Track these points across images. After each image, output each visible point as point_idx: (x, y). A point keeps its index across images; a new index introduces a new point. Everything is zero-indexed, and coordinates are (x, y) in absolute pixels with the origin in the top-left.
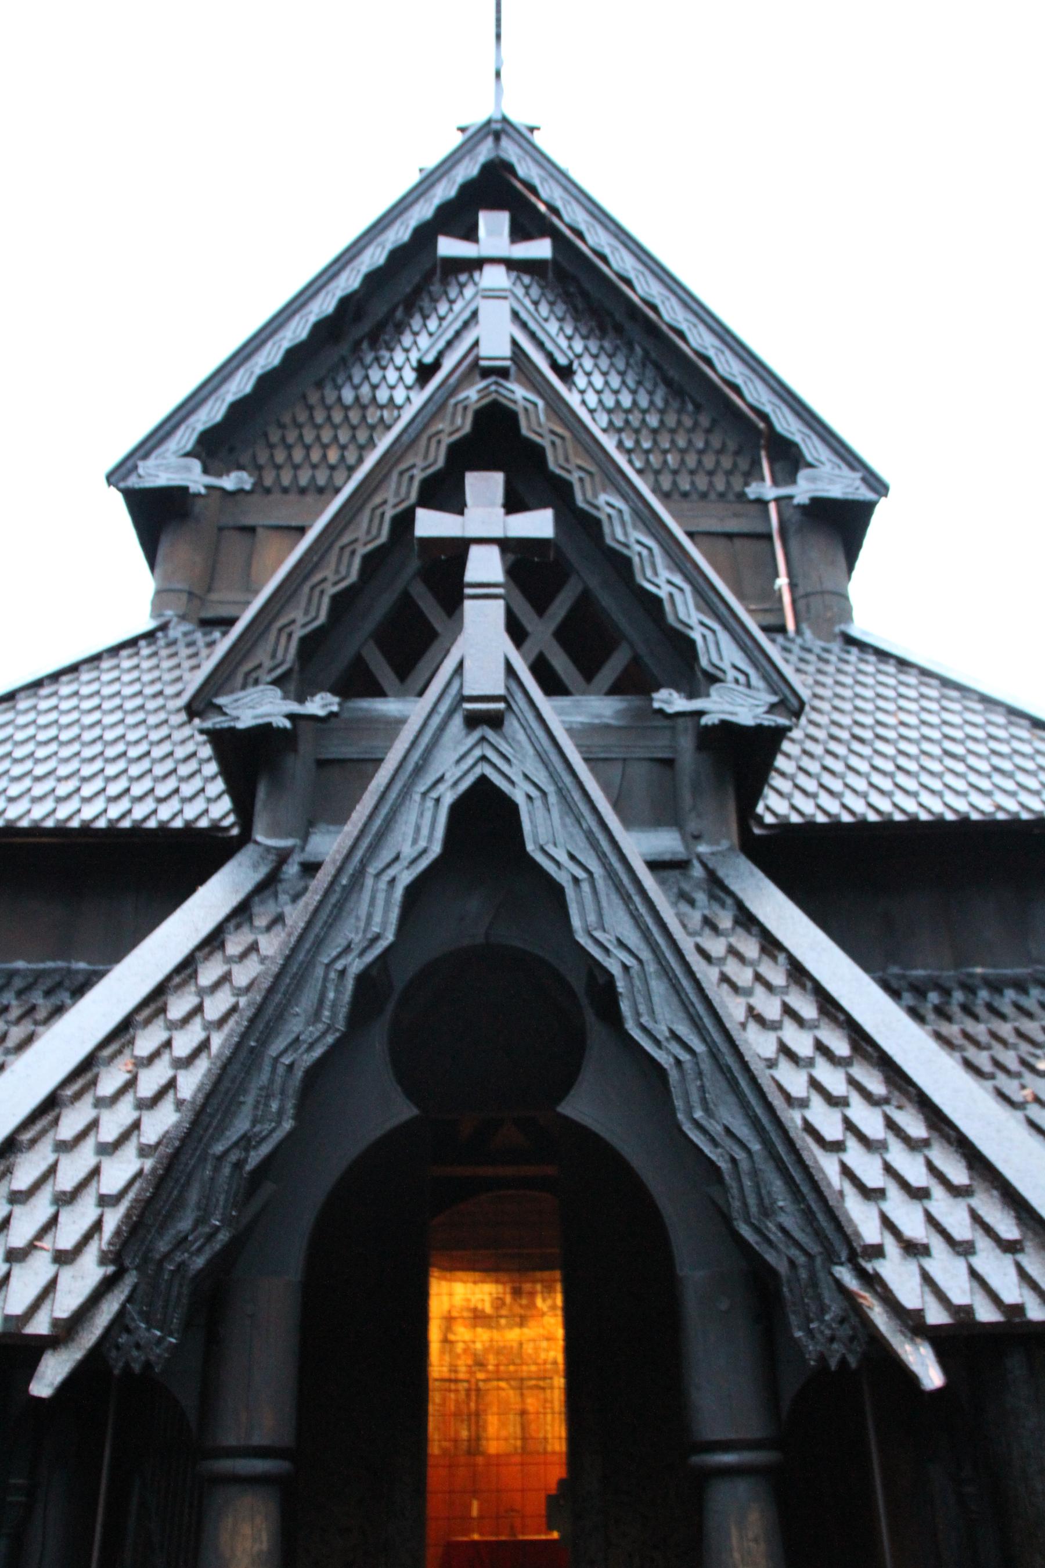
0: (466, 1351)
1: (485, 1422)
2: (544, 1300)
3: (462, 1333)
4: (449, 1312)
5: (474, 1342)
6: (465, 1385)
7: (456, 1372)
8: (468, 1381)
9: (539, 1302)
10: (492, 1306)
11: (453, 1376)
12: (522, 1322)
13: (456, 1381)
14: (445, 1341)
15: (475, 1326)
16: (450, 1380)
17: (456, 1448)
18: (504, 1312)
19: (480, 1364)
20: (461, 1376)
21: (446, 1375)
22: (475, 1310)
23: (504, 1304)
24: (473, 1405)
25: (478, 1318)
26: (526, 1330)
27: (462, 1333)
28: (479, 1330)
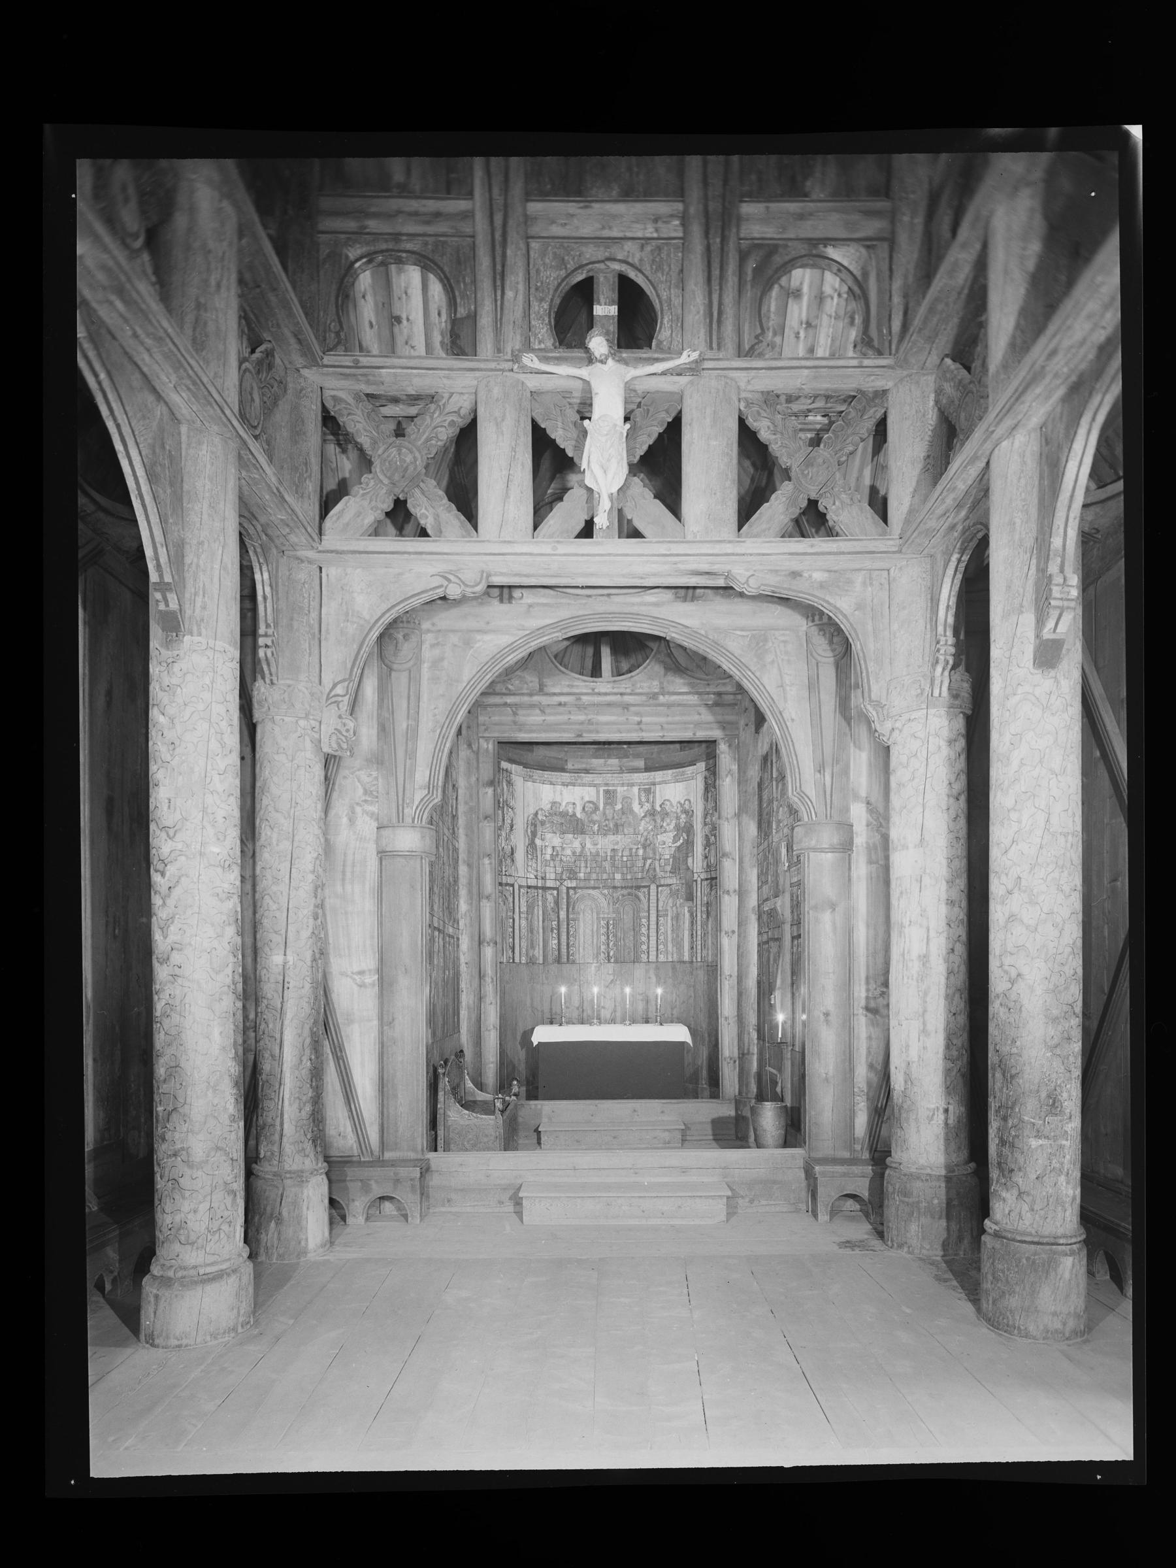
0: (553, 858)
2: (641, 804)
3: (551, 840)
4: (536, 814)
5: (563, 849)
6: (555, 892)
9: (636, 807)
12: (617, 829)
13: (544, 888)
14: (532, 844)
16: (536, 888)
17: (545, 957)
18: (595, 817)
19: (573, 874)
20: (549, 884)
21: (532, 882)
22: (564, 814)
23: (597, 808)
24: (563, 914)
27: (551, 840)
28: (571, 836)
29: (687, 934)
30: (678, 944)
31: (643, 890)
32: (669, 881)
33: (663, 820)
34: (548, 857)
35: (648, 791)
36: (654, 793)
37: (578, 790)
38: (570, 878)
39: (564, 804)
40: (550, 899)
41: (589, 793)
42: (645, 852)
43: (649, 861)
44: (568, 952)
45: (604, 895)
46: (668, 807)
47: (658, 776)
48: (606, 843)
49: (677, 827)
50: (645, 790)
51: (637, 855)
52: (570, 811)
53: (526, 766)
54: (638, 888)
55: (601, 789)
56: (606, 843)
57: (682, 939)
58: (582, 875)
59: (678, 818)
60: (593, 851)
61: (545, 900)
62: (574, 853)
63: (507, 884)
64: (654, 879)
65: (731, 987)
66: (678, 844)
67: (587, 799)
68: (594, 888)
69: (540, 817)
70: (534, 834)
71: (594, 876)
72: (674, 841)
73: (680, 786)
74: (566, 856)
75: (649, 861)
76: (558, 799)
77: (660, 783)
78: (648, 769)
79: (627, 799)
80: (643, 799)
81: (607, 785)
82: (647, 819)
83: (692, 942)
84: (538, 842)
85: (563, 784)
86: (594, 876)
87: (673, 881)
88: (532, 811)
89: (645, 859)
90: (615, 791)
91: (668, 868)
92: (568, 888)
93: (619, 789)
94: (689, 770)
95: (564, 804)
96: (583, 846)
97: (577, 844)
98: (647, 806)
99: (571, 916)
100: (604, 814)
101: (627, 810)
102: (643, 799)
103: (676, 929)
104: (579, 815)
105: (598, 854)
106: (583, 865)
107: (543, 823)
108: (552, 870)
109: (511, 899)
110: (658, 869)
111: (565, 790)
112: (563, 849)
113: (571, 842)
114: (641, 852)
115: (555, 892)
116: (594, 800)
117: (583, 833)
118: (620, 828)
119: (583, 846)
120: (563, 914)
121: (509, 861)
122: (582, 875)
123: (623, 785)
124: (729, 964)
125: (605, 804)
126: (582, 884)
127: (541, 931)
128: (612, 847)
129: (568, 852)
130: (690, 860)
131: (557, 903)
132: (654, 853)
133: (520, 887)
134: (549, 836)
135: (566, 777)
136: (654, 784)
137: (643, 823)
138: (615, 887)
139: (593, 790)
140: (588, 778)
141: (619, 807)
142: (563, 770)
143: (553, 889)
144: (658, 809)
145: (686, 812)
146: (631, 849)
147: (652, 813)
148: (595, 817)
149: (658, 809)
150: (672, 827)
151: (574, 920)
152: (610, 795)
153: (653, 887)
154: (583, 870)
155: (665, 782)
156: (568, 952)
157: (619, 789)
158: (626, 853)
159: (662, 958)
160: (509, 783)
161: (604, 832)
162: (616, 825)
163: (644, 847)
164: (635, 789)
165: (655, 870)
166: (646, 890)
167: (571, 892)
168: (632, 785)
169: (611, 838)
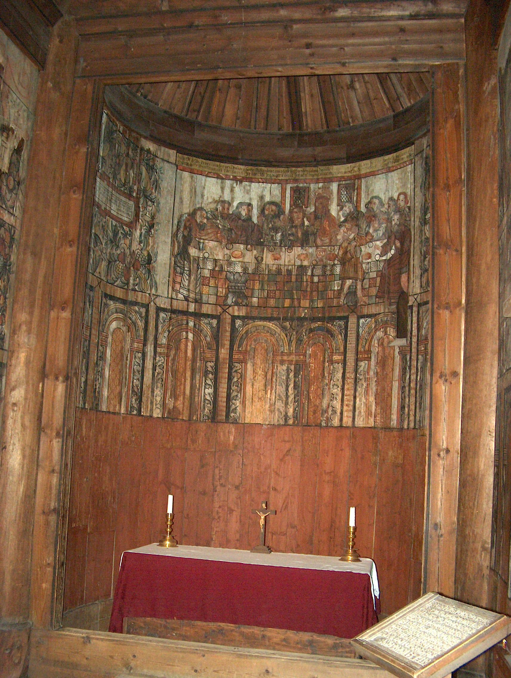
1: (243, 377)
2: (341, 206)
4: (192, 214)
5: (230, 263)
6: (214, 322)
7: (198, 301)
8: (218, 318)
9: (334, 210)
10: (262, 211)
11: (192, 308)
13: (198, 315)
15: (232, 242)
16: (185, 313)
19: (241, 295)
20: (206, 309)
21: (179, 305)
23: (280, 211)
24: (224, 352)
25: (239, 229)
26: (311, 250)
27: (213, 250)
28: (242, 246)
29: (396, 385)
30: (383, 399)
31: (337, 323)
32: (373, 310)
33: (369, 226)
34: (206, 273)
35: (351, 185)
36: (359, 188)
37: (256, 189)
38: (236, 304)
39: (235, 204)
40: (207, 330)
41: (270, 192)
42: (343, 270)
43: (348, 282)
44: (228, 407)
45: (284, 328)
46: (376, 207)
47: (365, 166)
48: (290, 258)
49: (390, 236)
50: (346, 187)
51: (332, 274)
52: (244, 213)
53: (181, 150)
54: (332, 319)
55: (289, 187)
56: (290, 258)
57: (390, 395)
58: (255, 300)
59: (389, 220)
60: (274, 268)
61: (197, 331)
62: (245, 269)
63: (136, 303)
64: (354, 308)
65: (448, 472)
66: (389, 255)
67: (267, 199)
68: (270, 319)
69: (198, 221)
70: (187, 241)
71: (272, 302)
72: (384, 252)
73: (395, 176)
74: (234, 274)
75: (348, 282)
76: (227, 197)
77: (367, 175)
78: (351, 159)
79: (323, 201)
80: (344, 199)
81: (296, 181)
82: (348, 225)
83: (403, 399)
84: (193, 252)
85: (235, 179)
86: (272, 302)
87: (381, 309)
88: (187, 209)
89: (343, 279)
90: (309, 188)
91: (374, 291)
92: (234, 318)
93: (312, 186)
94: (405, 153)
95: (235, 204)
96: (259, 260)
97: (250, 257)
98: (348, 208)
99: (236, 356)
100: (291, 220)
101: (322, 213)
102: (344, 199)
103: (383, 378)
104: (255, 220)
105: (279, 272)
106: (257, 286)
107: (202, 227)
108: (212, 291)
109: (141, 324)
110: (359, 293)
111: (238, 189)
112: (230, 263)
113: (243, 255)
114: (338, 270)
115: (214, 322)
116: (278, 199)
117: (260, 244)
118: (311, 238)
119: (259, 260)
120: (224, 352)
121: (142, 271)
122: (255, 300)
123: (317, 181)
124: (447, 433)
125: (294, 204)
126: (255, 313)
127: (188, 374)
128: (298, 263)
129: (238, 269)
130: (404, 278)
131: (217, 336)
132: (356, 272)
133: (159, 310)
134: (212, 244)
135: (240, 170)
136: (359, 177)
137: (343, 229)
138: (300, 319)
139: (276, 189)
140: (273, 172)
141: (312, 209)
142: (234, 160)
143: (212, 317)
144: (363, 209)
145: (398, 210)
146: (325, 266)
147: (354, 218)
148: (279, 224)
149: (363, 209)
150: (381, 233)
151: (240, 362)
152: (299, 195)
153: (352, 320)
154: (256, 293)
155: (373, 174)
156: (228, 407)
157: (312, 186)
158: (318, 271)
159: (360, 422)
160: (151, 169)
161: (289, 244)
162: (306, 234)
163: (343, 263)
164: (334, 187)
165: (355, 293)
166: (342, 323)
167: (238, 323)
168: (331, 180)
169: (298, 250)
